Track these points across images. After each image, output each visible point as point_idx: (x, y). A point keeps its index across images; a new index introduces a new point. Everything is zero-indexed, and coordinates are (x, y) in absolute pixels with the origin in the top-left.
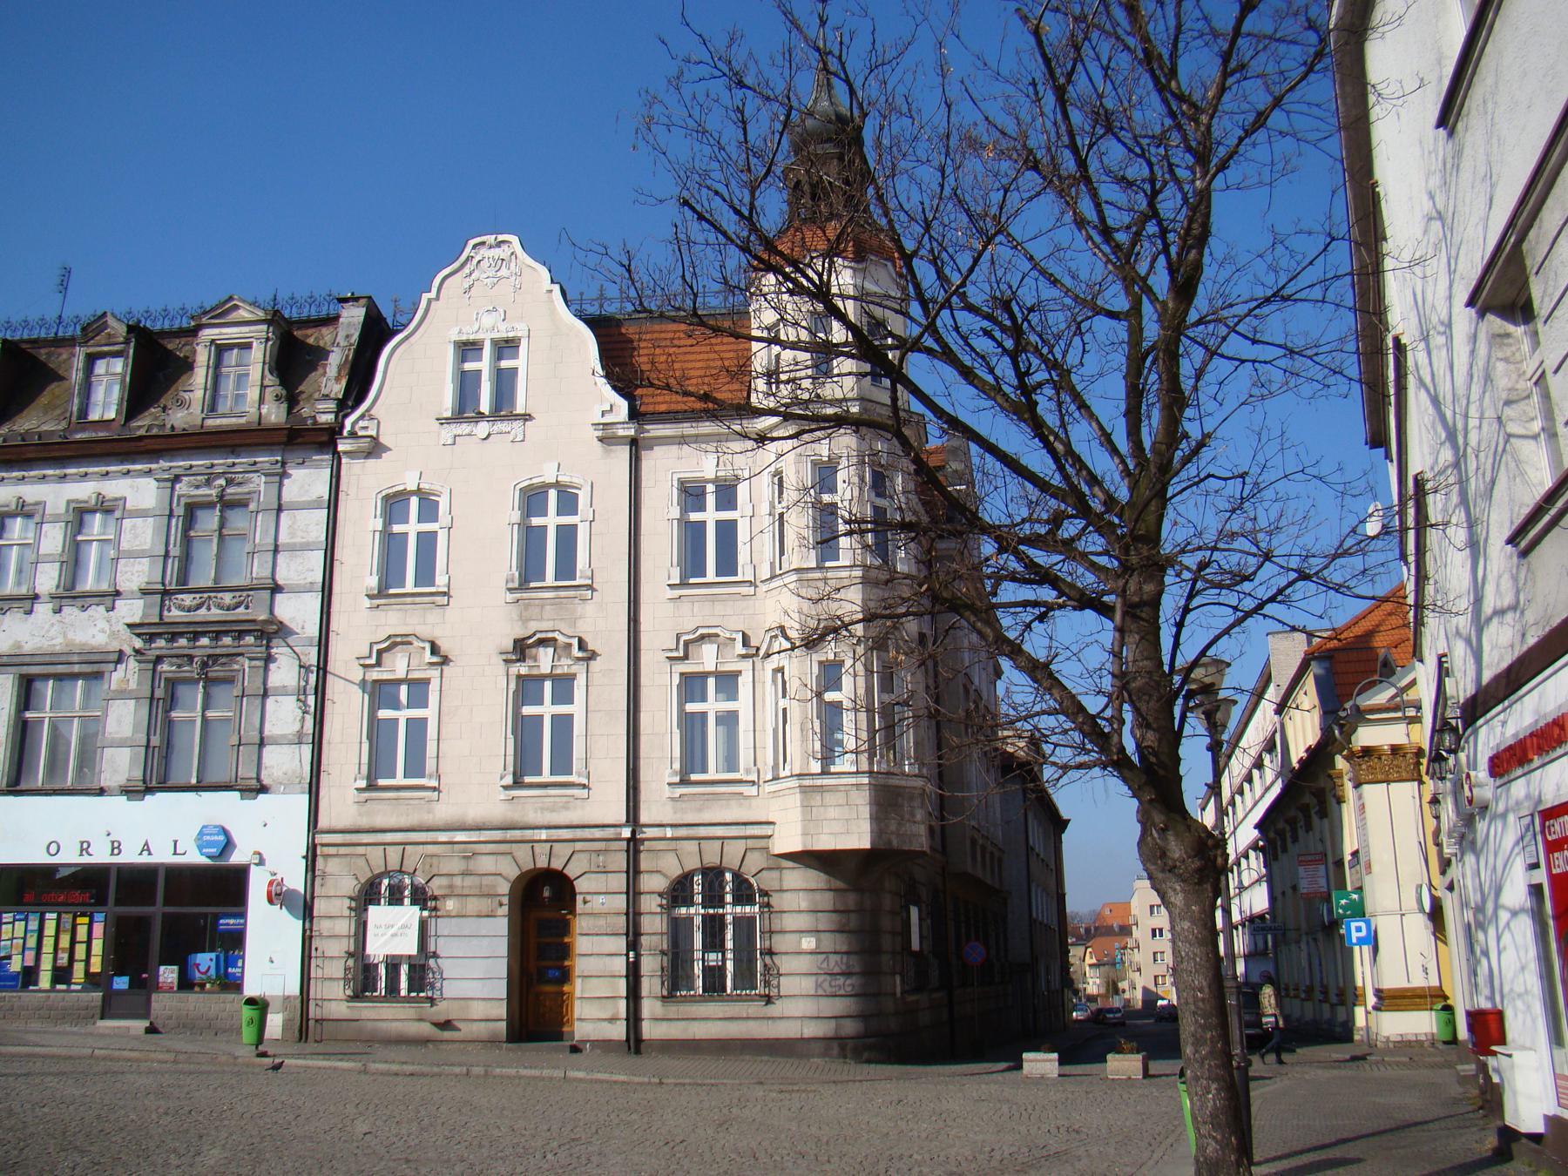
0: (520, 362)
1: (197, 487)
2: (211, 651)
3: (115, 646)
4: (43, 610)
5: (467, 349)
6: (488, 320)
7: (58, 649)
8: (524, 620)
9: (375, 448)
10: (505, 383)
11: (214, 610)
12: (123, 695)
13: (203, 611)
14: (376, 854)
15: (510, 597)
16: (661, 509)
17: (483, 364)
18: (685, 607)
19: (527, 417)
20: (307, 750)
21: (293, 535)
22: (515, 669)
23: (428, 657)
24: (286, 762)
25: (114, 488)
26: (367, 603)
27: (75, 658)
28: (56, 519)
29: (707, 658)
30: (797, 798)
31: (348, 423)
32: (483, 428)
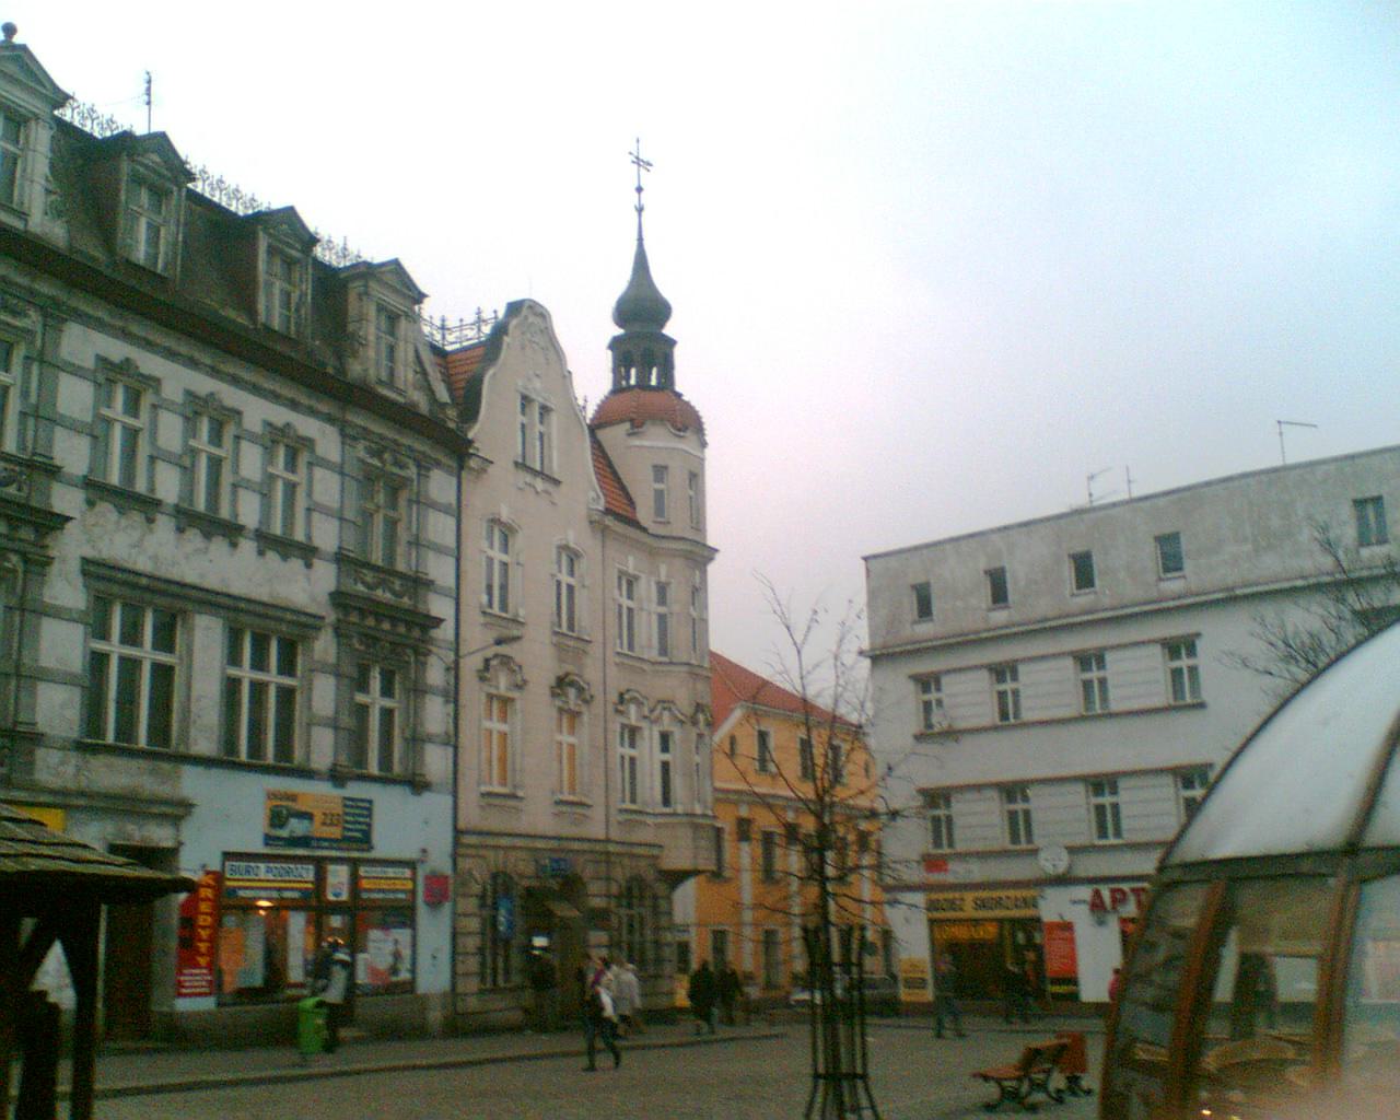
1: (372, 456)
2: (390, 638)
3: (312, 609)
7: (265, 599)
8: (561, 661)
11: (388, 595)
12: (324, 668)
13: (379, 592)
14: (490, 854)
15: (555, 639)
19: (557, 482)
20: (450, 750)
24: (436, 761)
26: (482, 619)
27: (289, 616)
30: (689, 832)
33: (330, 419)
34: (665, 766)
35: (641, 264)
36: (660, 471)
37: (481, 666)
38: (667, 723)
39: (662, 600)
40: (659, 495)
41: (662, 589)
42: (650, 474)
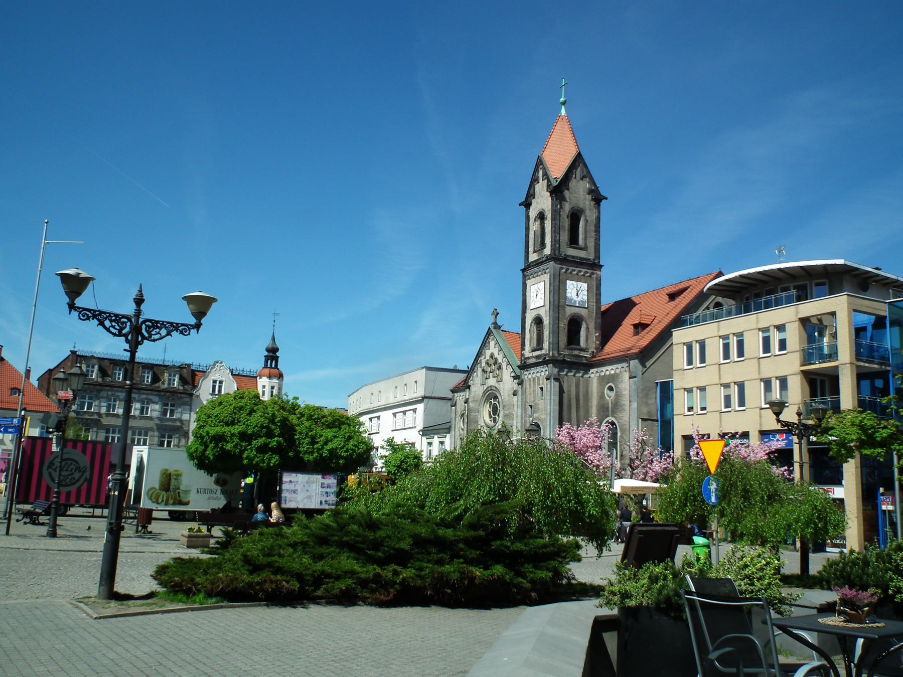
5: (215, 382)
10: (220, 387)
25: (151, 397)
33: (155, 395)
36: (264, 387)
42: (262, 387)
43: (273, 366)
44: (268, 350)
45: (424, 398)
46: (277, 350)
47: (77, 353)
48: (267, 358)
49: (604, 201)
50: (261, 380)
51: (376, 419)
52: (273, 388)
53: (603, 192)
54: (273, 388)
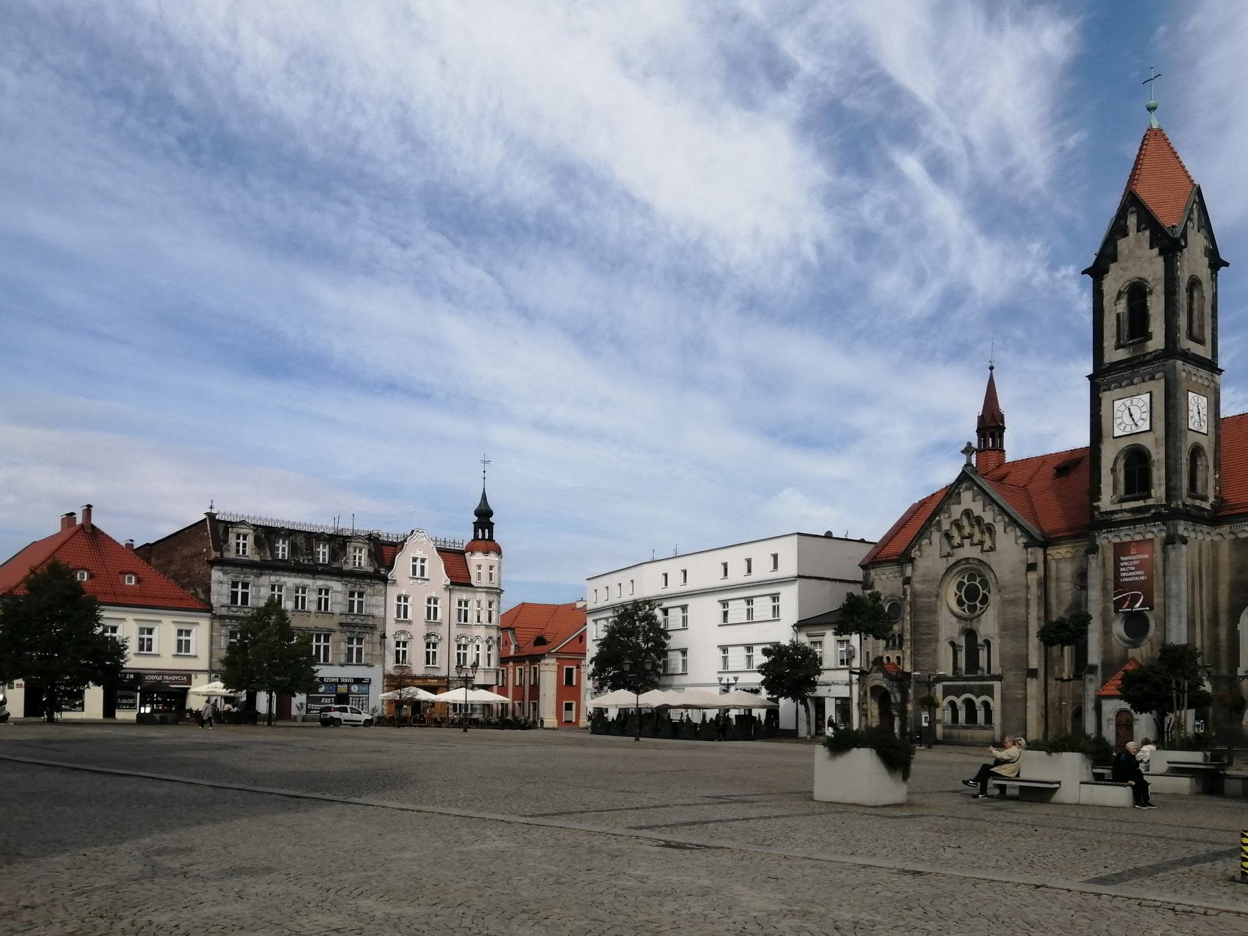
0: (426, 564)
4: (312, 617)
5: (415, 560)
6: (419, 552)
8: (428, 629)
9: (394, 582)
10: (422, 568)
16: (455, 606)
17: (418, 563)
18: (459, 629)
19: (428, 580)
21: (376, 602)
22: (426, 641)
23: (409, 636)
28: (314, 590)
29: (463, 641)
31: (389, 575)
32: (419, 581)
33: (337, 581)
34: (478, 655)
35: (484, 497)
37: (394, 634)
38: (477, 643)
39: (479, 607)
40: (479, 573)
41: (479, 602)
42: (476, 568)
43: (487, 537)
44: (477, 513)
45: (799, 577)
46: (490, 513)
47: (217, 517)
48: (477, 526)
49: (1222, 269)
50: (473, 558)
51: (679, 610)
52: (491, 568)
53: (1223, 256)
54: (491, 568)
